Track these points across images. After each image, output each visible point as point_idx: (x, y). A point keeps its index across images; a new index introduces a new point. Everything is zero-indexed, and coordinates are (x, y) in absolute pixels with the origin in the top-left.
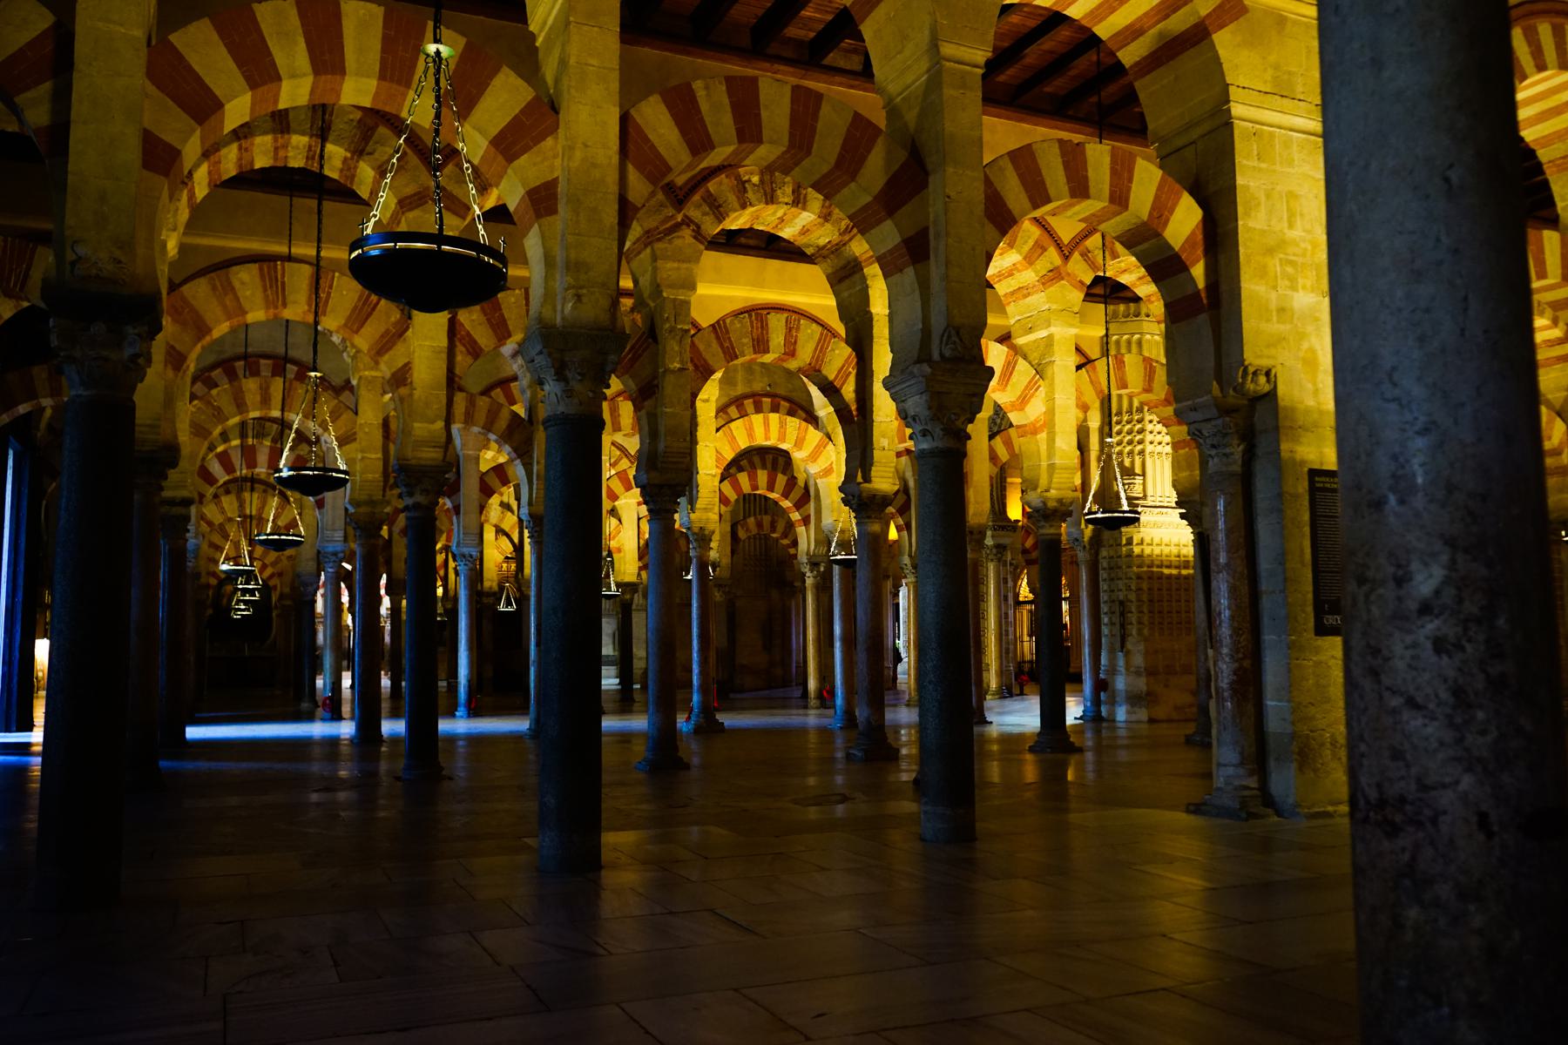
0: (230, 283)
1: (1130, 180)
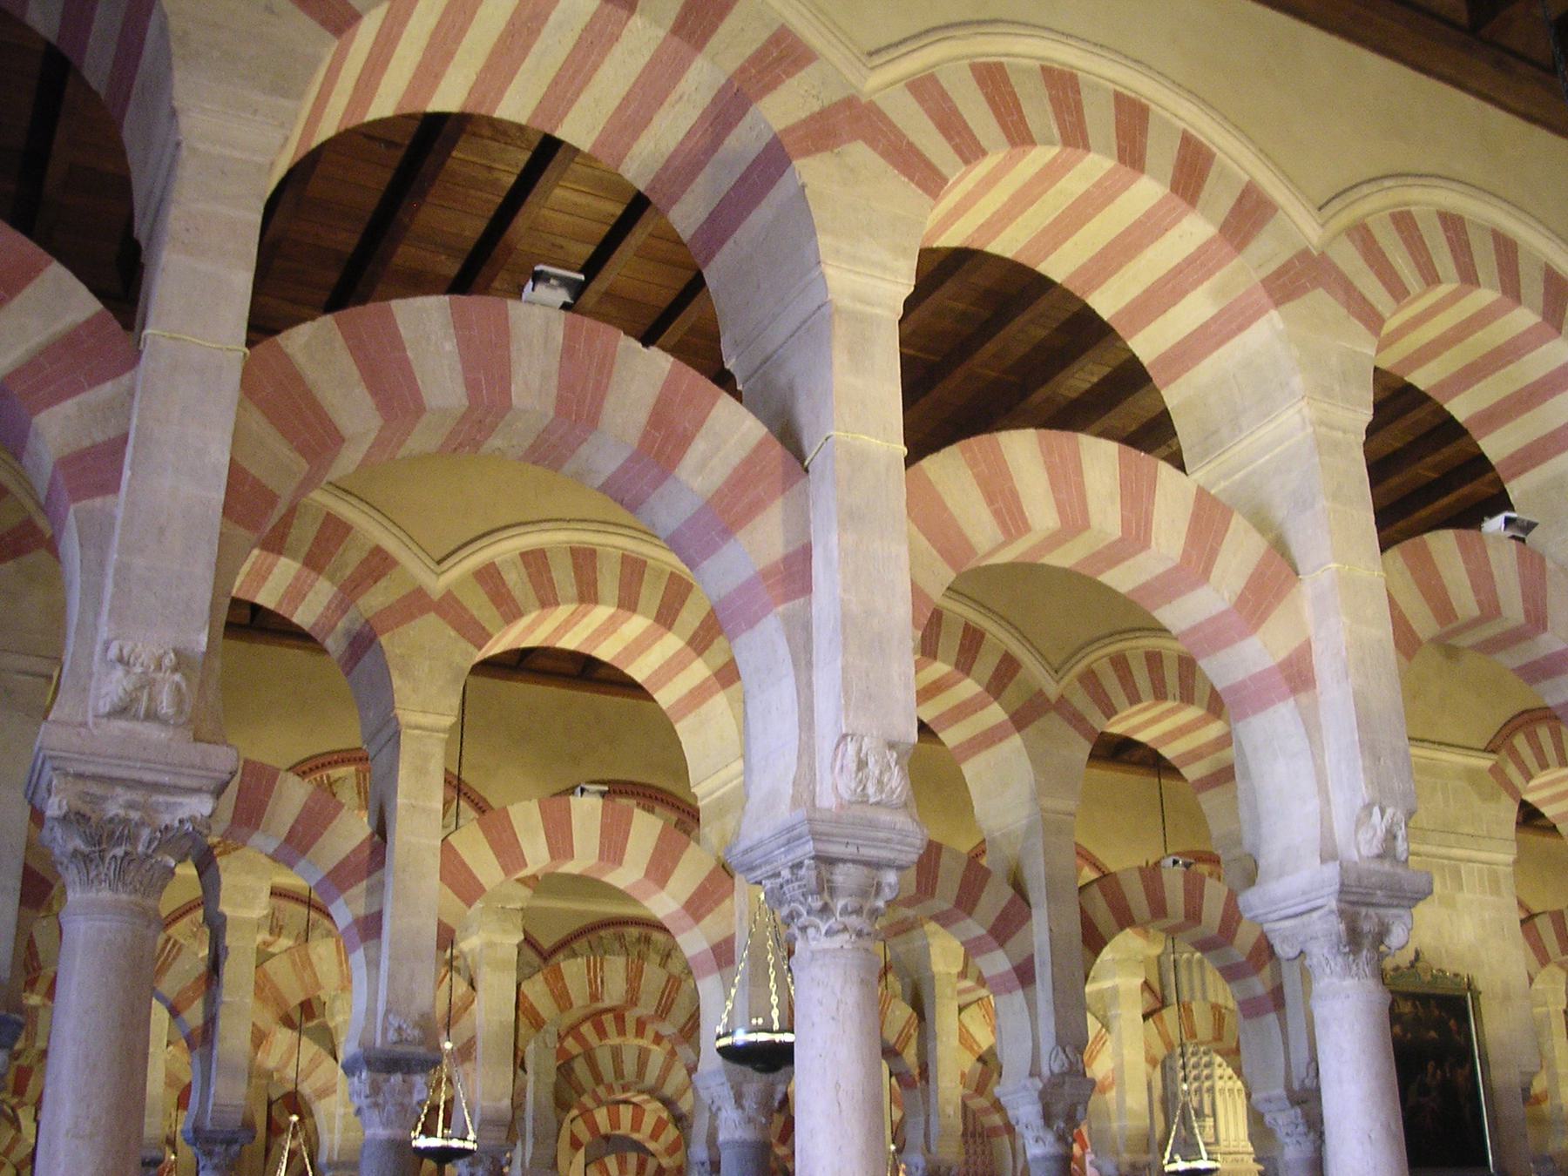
0: (309, 959)
1: (1202, 897)
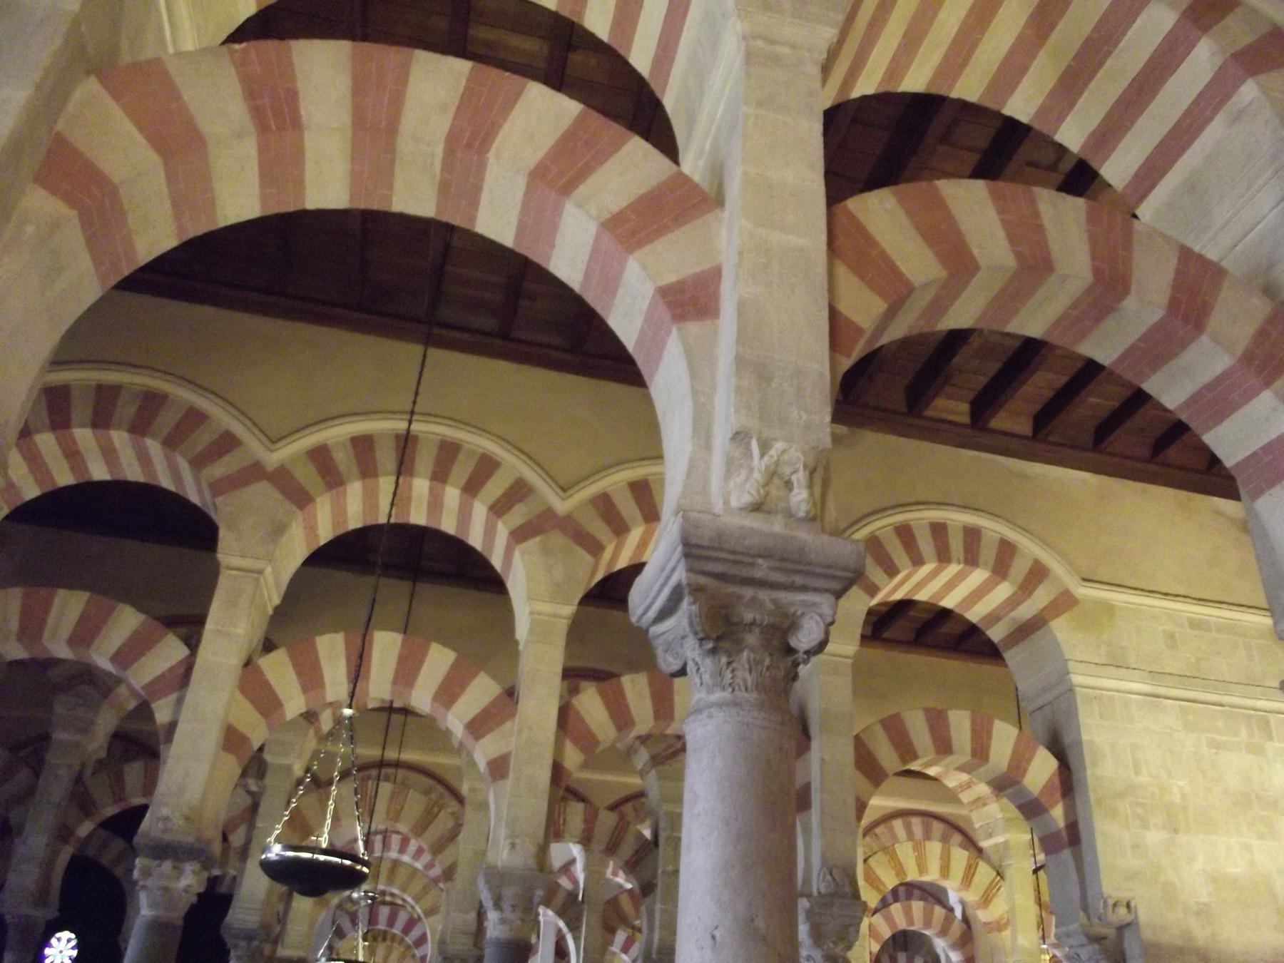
1: (989, 738)
